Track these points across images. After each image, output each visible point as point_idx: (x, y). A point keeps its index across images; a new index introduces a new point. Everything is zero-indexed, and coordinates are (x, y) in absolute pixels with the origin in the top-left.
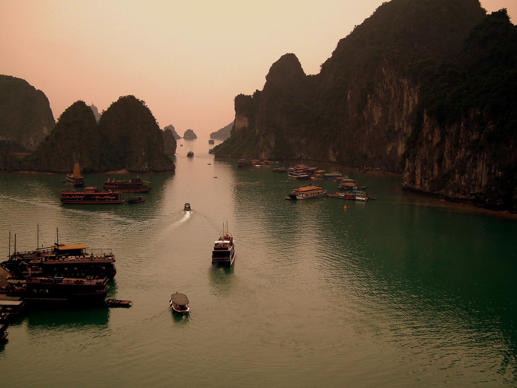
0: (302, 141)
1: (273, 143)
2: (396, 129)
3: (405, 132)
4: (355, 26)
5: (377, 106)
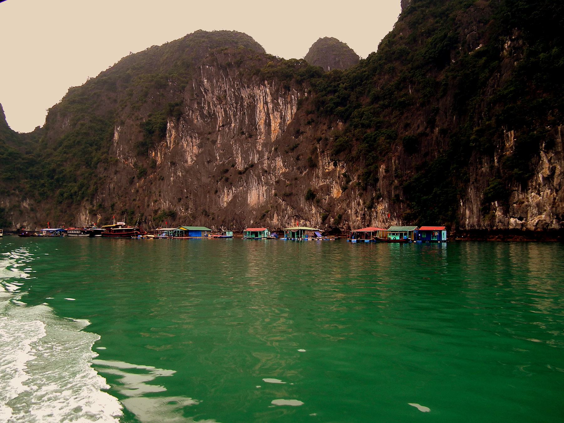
0: (24, 204)
2: (240, 167)
5: (191, 137)
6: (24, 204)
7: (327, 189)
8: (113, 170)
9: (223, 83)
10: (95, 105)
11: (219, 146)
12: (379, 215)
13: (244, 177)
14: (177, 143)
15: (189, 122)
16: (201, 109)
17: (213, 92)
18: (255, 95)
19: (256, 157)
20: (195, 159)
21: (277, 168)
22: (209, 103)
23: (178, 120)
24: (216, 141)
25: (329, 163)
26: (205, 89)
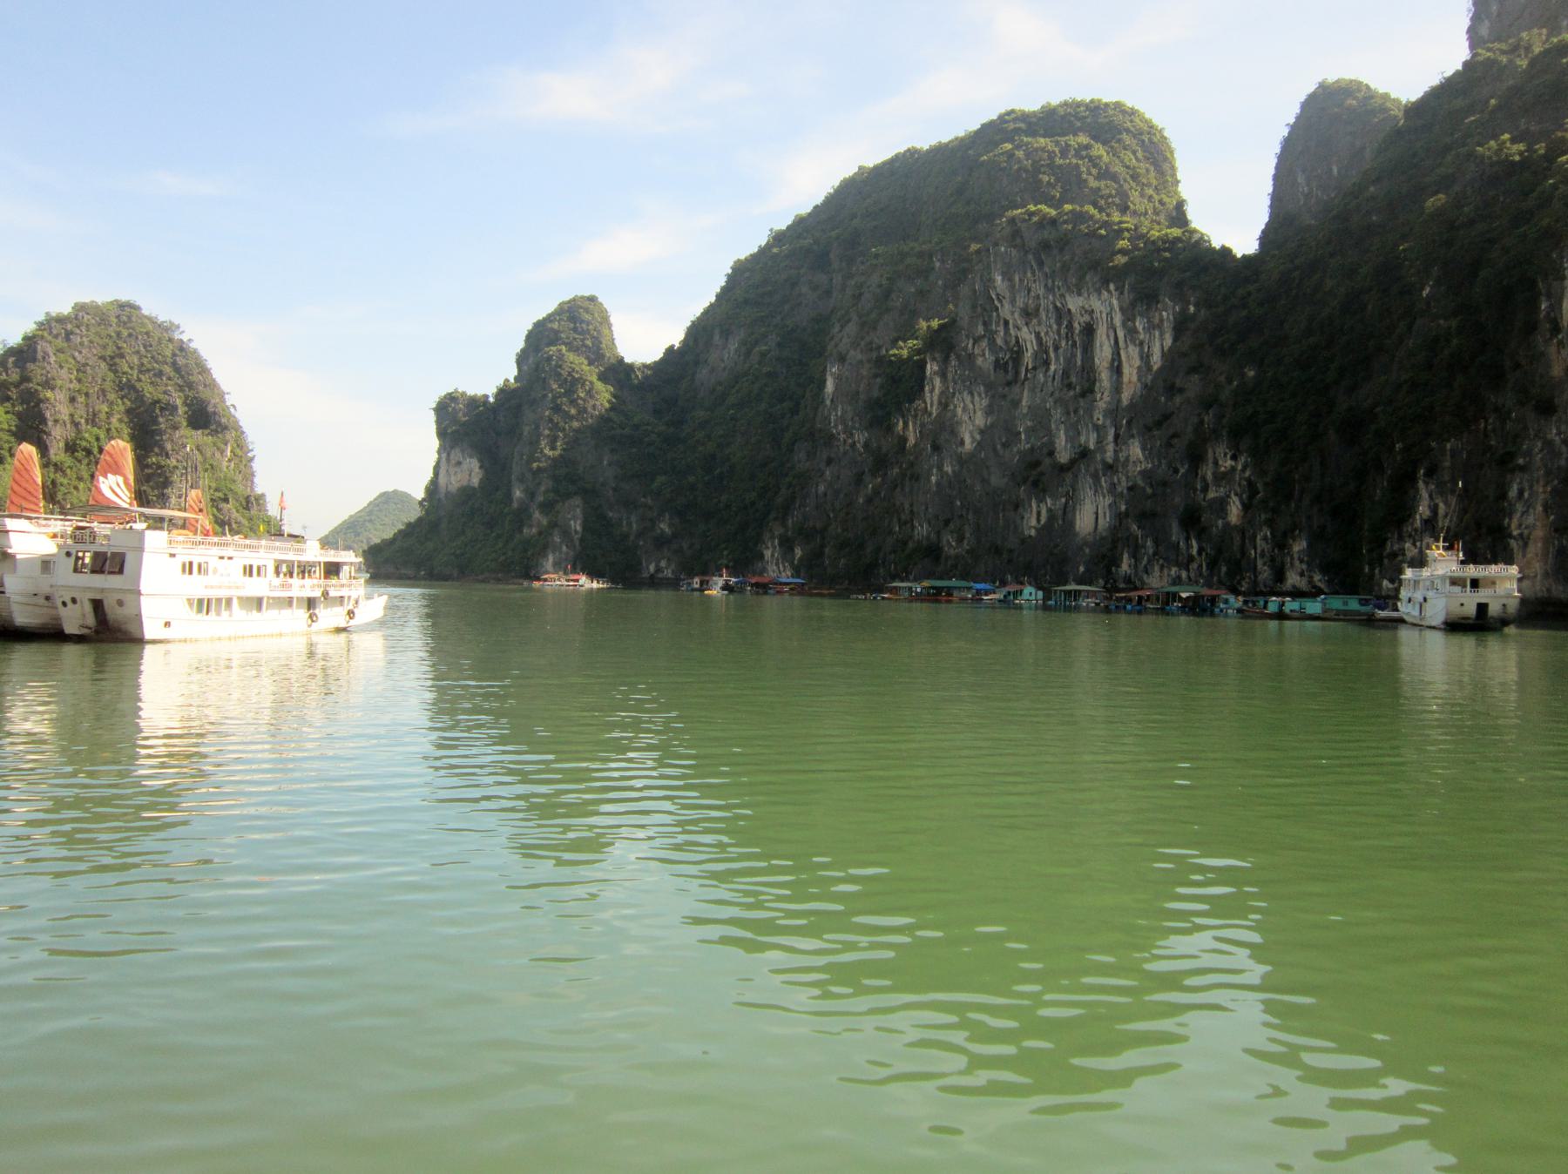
1: (576, 525)
2: (1063, 457)
3: (1110, 461)
4: (771, 230)
5: (972, 394)
6: (662, 526)
7: (1221, 506)
8: (825, 457)
9: (1035, 281)
10: (787, 307)
11: (1025, 411)
12: (1297, 563)
13: (1069, 477)
14: (944, 406)
16: (990, 336)
17: (1013, 302)
18: (1093, 311)
19: (1093, 438)
20: (978, 437)
21: (1131, 460)
22: (1006, 323)
23: (946, 360)
24: (1020, 401)
25: (1225, 455)
26: (998, 295)
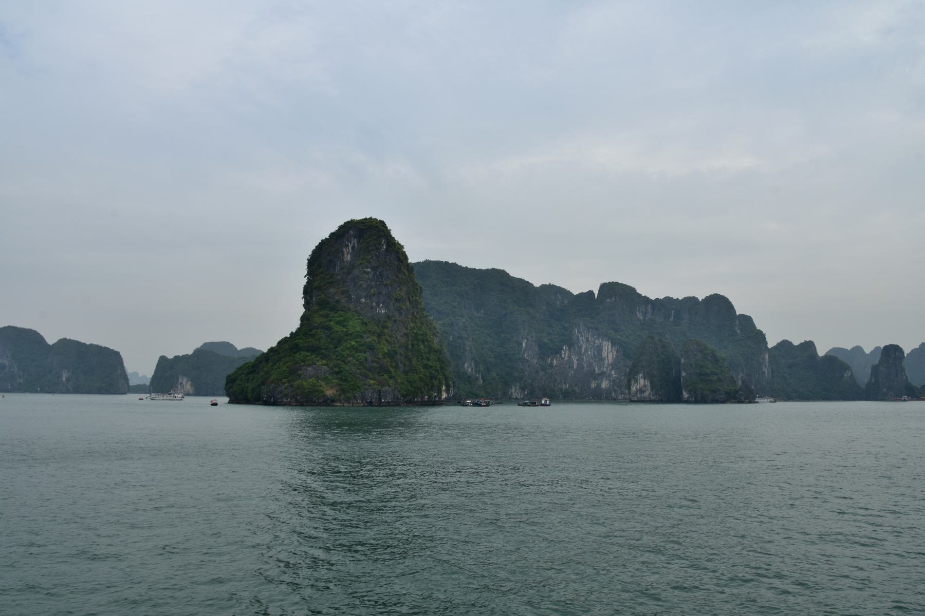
14: (570, 357)
15: (575, 348)
